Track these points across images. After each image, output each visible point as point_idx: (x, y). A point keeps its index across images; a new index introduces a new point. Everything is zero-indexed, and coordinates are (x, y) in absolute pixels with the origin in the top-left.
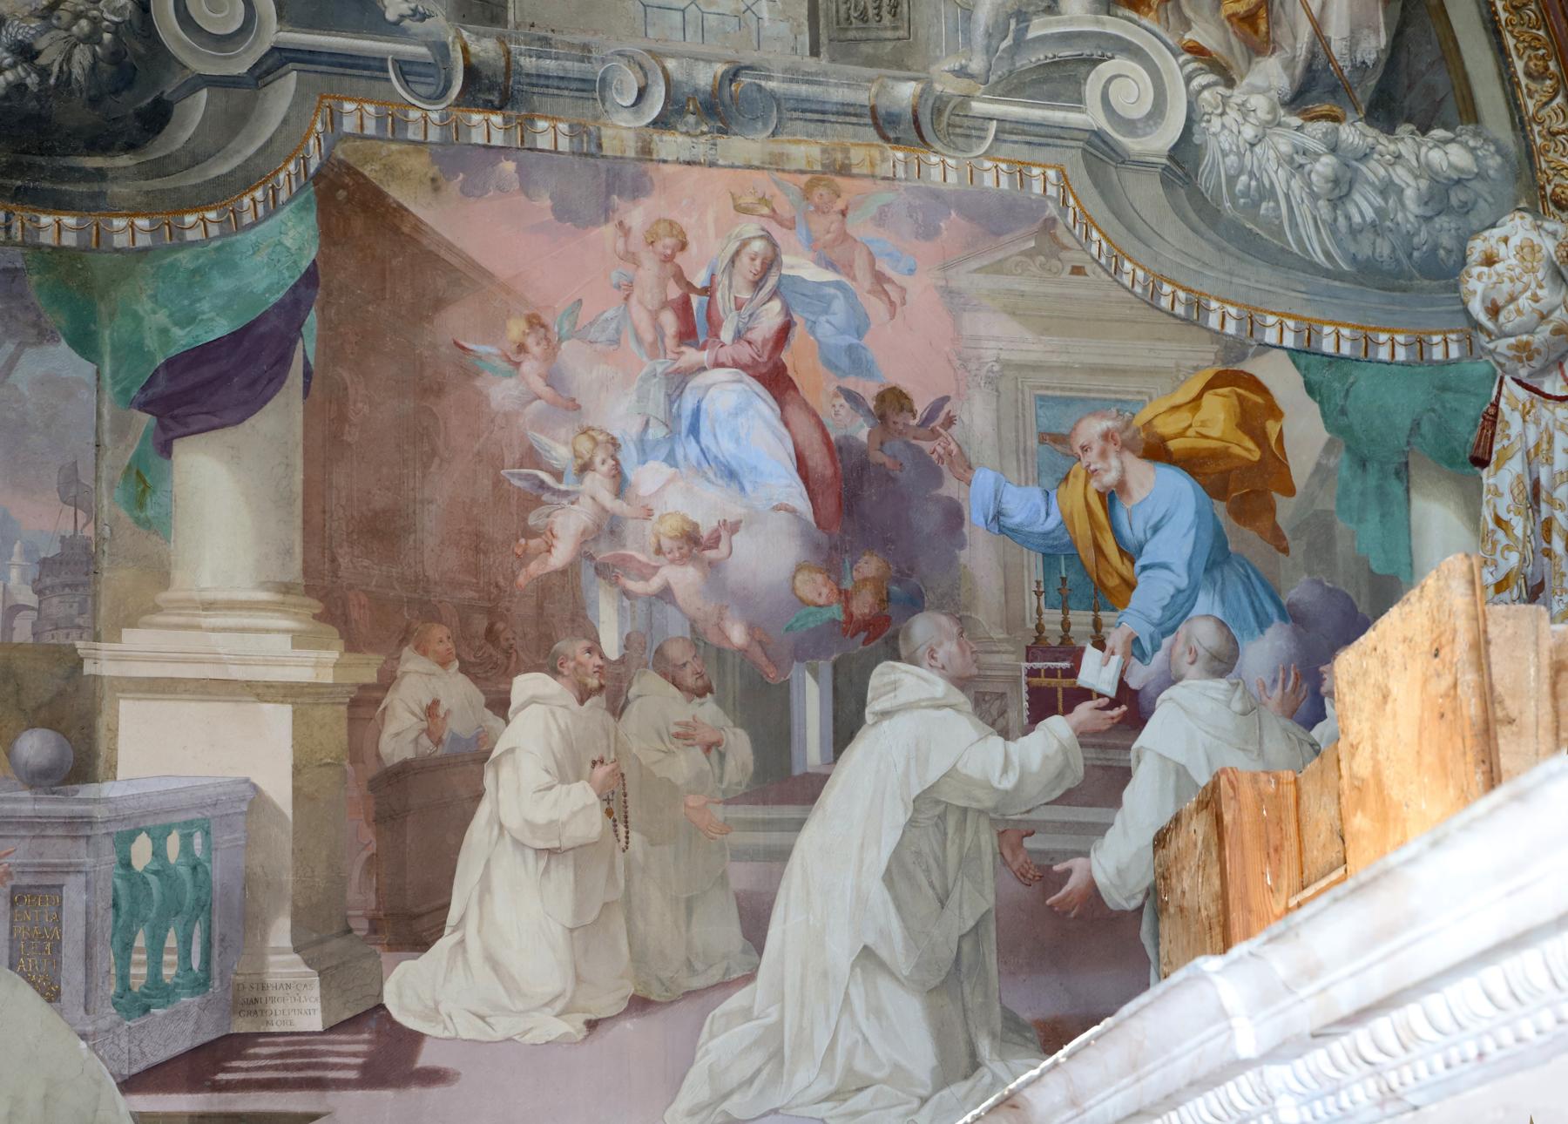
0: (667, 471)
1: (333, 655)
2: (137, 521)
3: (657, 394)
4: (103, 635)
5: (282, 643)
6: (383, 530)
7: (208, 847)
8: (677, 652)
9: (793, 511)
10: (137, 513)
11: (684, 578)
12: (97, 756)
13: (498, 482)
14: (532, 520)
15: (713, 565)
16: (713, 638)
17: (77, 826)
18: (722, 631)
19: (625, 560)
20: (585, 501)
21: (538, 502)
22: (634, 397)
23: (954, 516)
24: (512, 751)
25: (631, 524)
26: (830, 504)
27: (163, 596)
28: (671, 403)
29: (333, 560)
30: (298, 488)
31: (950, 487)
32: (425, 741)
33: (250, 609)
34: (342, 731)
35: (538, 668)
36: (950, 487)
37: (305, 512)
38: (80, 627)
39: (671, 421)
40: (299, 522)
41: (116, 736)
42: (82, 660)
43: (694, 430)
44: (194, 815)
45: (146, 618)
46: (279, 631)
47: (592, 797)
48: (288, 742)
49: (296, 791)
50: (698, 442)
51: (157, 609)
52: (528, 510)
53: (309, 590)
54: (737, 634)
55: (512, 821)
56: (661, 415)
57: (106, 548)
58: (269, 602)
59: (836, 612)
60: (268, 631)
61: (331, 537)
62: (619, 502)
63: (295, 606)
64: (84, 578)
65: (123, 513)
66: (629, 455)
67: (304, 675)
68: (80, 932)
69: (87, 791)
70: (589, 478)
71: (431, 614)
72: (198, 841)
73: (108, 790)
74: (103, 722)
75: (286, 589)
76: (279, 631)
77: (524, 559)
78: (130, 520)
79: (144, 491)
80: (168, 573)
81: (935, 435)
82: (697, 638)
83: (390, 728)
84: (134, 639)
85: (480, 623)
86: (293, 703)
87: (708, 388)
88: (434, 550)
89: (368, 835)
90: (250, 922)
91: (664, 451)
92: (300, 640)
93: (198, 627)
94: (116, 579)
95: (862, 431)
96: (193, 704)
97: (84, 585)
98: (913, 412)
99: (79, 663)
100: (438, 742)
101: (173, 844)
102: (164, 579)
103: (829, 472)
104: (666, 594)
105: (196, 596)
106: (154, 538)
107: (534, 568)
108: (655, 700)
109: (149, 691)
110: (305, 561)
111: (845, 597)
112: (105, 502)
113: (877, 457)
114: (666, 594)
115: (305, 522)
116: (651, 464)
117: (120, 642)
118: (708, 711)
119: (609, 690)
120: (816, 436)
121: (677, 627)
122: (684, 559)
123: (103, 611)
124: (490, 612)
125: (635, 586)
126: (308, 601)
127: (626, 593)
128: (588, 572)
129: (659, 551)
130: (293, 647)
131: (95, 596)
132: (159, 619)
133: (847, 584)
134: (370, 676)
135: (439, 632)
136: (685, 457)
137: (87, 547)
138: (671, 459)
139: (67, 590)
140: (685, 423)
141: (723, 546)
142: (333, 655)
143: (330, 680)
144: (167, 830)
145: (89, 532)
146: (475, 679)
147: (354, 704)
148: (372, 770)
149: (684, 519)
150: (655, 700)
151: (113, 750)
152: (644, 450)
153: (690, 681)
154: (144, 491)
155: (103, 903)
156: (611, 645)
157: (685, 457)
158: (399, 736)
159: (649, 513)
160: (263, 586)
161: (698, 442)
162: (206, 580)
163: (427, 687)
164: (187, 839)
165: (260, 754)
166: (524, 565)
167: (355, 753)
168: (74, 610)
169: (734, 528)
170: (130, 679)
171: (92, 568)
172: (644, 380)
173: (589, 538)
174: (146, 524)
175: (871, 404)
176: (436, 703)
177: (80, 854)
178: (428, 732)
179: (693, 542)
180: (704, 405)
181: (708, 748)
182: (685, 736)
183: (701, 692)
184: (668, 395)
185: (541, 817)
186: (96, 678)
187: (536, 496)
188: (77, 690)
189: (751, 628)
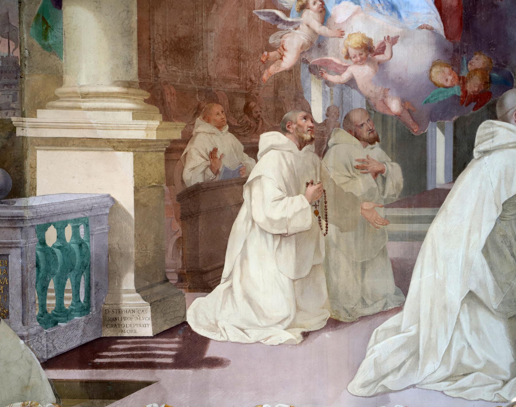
0: (353, 7)
1: (156, 124)
2: (44, 47)
4: (26, 114)
5: (127, 117)
6: (184, 49)
7: (88, 233)
8: (358, 118)
9: (431, 29)
10: (43, 42)
11: (363, 73)
12: (25, 182)
13: (251, 18)
14: (272, 40)
15: (381, 64)
16: (380, 108)
17: (16, 222)
18: (384, 103)
19: (327, 63)
20: (303, 27)
21: (275, 29)
24: (259, 177)
25: (331, 40)
26: (455, 23)
27: (59, 91)
29: (155, 67)
30: (135, 25)
32: (209, 172)
33: (108, 97)
34: (162, 167)
35: (275, 129)
37: (139, 40)
38: (13, 109)
40: (135, 45)
41: (35, 171)
42: (15, 127)
44: (79, 215)
45: (50, 103)
46: (125, 110)
47: (307, 204)
48: (132, 173)
49: (137, 202)
51: (56, 98)
52: (269, 34)
53: (142, 86)
54: (395, 106)
55: (260, 218)
57: (26, 63)
58: (118, 93)
59: (457, 91)
60: (118, 110)
61: (154, 54)
63: (134, 95)
64: (14, 81)
65: (36, 43)
67: (140, 135)
68: (19, 281)
69: (20, 202)
70: (306, 12)
71: (213, 99)
72: (82, 230)
73: (32, 201)
74: (28, 162)
75: (129, 85)
76: (125, 110)
77: (266, 64)
78: (40, 46)
79: (46, 29)
80: (62, 77)
82: (370, 109)
83: (189, 165)
84: (44, 115)
85: (241, 103)
86: (133, 151)
88: (213, 61)
89: (177, 226)
90: (112, 276)
92: (137, 115)
93: (80, 108)
94: (33, 81)
96: (78, 153)
97: (15, 84)
99: (14, 129)
100: (217, 173)
101: (68, 232)
102: (60, 81)
104: (351, 82)
105: (78, 90)
106: (53, 57)
107: (273, 69)
108: (345, 147)
109: (53, 145)
110: (139, 68)
111: (463, 81)
112: (25, 36)
114: (351, 82)
115: (139, 45)
117: (36, 117)
118: (376, 152)
119: (317, 141)
121: (358, 102)
122: (363, 61)
123: (26, 99)
124: (247, 96)
125: (333, 78)
126: (141, 92)
127: (327, 83)
128: (304, 70)
129: (348, 56)
130: (133, 119)
131: (22, 90)
132: (58, 104)
133: (464, 73)
134: (177, 135)
135: (217, 108)
137: (15, 63)
139: (6, 88)
141: (387, 52)
142: (156, 124)
143: (154, 138)
144: (65, 224)
145: (17, 53)
146: (238, 136)
147: (168, 151)
148: (179, 189)
149: (364, 37)
150: (345, 147)
151: (34, 179)
153: (365, 134)
154: (46, 29)
155: (31, 265)
156: (318, 114)
158: (194, 170)
159: (342, 34)
160: (115, 83)
162: (83, 81)
163: (210, 142)
164: (76, 229)
165: (115, 180)
166: (267, 67)
167: (170, 180)
168: (10, 100)
169: (394, 41)
170: (42, 138)
171: (19, 74)
173: (305, 51)
174: (48, 48)
176: (215, 150)
177: (18, 237)
178: (211, 167)
179: (368, 50)
181: (376, 175)
182: (362, 167)
183: (372, 141)
185: (276, 215)
186: (23, 137)
187: (274, 25)
188: (13, 145)
189: (403, 102)
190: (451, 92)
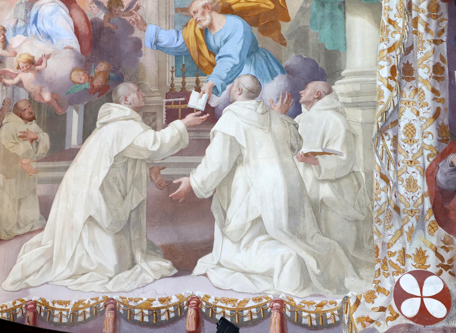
0: (23, 38)
3: (22, 10)
8: (22, 105)
9: (72, 48)
11: (28, 77)
15: (39, 71)
16: (37, 99)
18: (40, 95)
22: (13, 12)
23: (138, 44)
25: (8, 59)
26: (87, 45)
28: (27, 13)
31: (137, 33)
36: (137, 33)
39: (26, 20)
43: (35, 22)
50: (36, 26)
54: (47, 97)
56: (23, 17)
59: (87, 85)
62: (4, 51)
66: (9, 34)
81: (132, 14)
82: (31, 100)
87: (41, 5)
91: (23, 30)
95: (101, 15)
98: (123, 6)
103: (87, 32)
104: (20, 84)
111: (91, 79)
113: (107, 25)
114: (20, 84)
116: (18, 36)
118: (33, 127)
120: (83, 20)
121: (23, 95)
122: (28, 70)
127: (4, 84)
129: (18, 68)
133: (92, 75)
136: (31, 32)
138: (25, 34)
140: (32, 20)
141: (44, 64)
149: (29, 55)
152: (15, 31)
153: (27, 115)
157: (31, 32)
159: (15, 54)
161: (36, 26)
169: (48, 57)
172: (17, 5)
175: (106, 5)
179: (32, 63)
180: (39, 12)
181: (32, 141)
182: (23, 137)
183: (30, 120)
184: (26, 10)
189: (53, 94)
190: (83, 87)
